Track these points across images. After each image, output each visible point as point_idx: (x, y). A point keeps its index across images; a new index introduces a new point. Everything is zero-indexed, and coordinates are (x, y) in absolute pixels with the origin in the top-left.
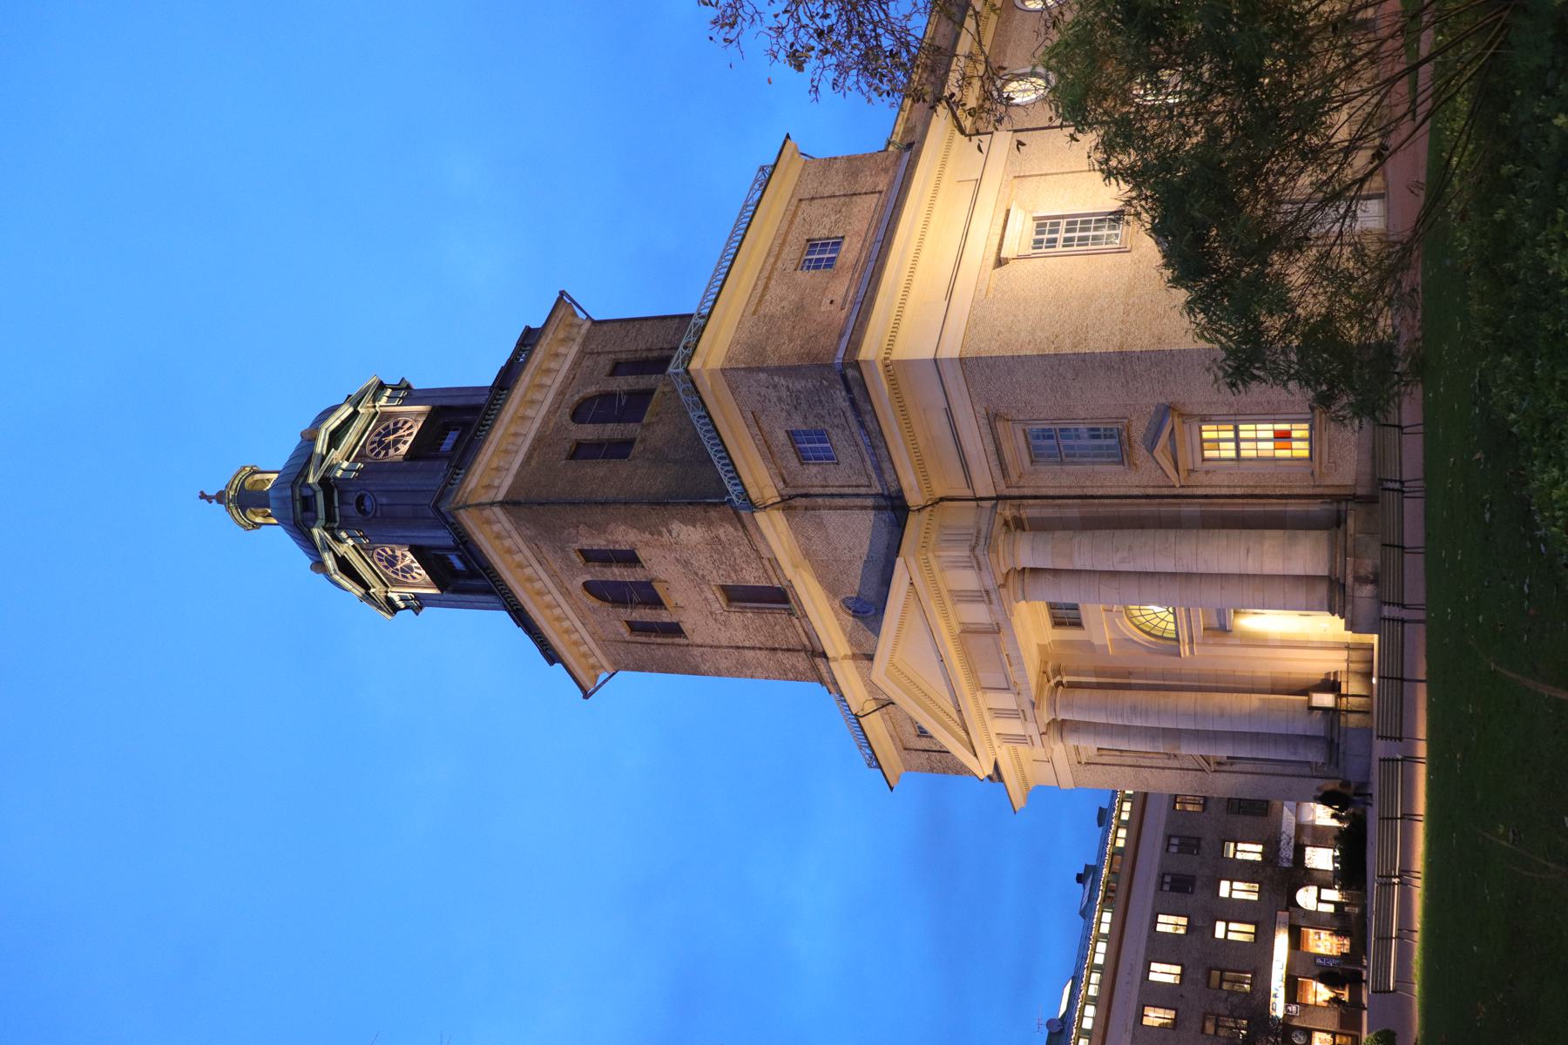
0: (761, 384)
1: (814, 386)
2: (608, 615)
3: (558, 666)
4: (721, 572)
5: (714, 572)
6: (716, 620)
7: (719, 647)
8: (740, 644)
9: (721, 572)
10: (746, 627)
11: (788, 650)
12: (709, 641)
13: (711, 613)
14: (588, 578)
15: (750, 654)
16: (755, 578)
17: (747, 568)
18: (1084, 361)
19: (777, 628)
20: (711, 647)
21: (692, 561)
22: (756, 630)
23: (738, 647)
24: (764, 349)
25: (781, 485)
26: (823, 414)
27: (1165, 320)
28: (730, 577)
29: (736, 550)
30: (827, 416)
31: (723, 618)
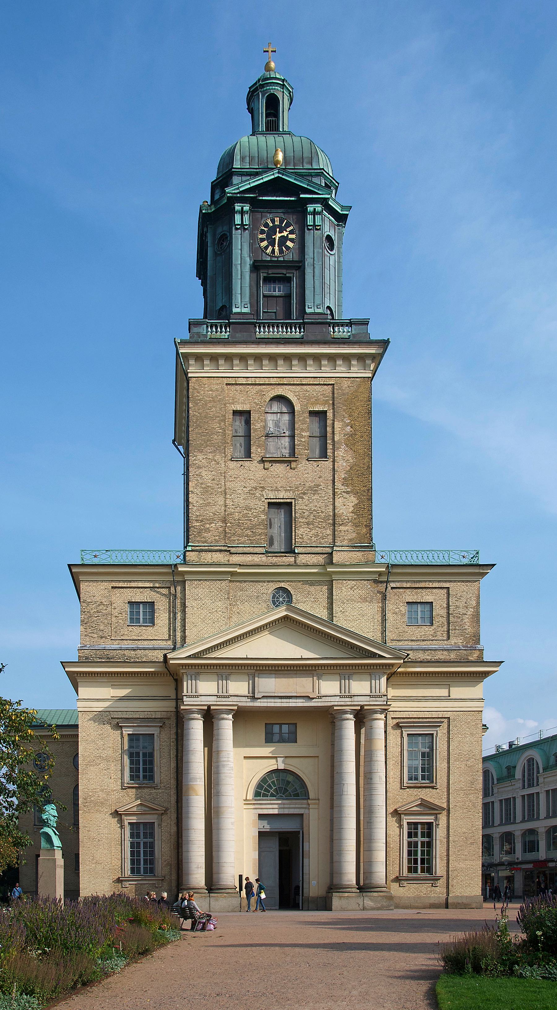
0: (469, 600)
1: (465, 629)
2: (255, 403)
8: (228, 496)
10: (248, 508)
14: (297, 408)
16: (302, 535)
17: (311, 533)
21: (316, 497)
22: (245, 516)
23: (226, 494)
25: (393, 585)
26: (444, 628)
28: (303, 517)
30: (442, 630)
31: (257, 495)
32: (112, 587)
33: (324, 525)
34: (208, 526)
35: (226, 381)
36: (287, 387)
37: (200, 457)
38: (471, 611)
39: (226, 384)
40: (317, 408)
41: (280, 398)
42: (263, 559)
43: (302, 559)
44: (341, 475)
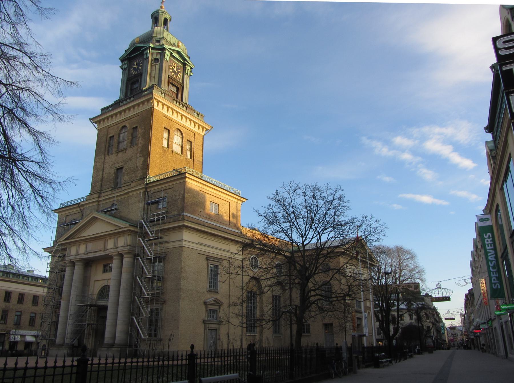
3: (100, 112)
4: (127, 169)
5: (127, 167)
6: (113, 165)
7: (104, 164)
8: (104, 170)
9: (127, 169)
10: (110, 173)
11: (101, 185)
12: (106, 161)
13: (115, 164)
15: (101, 173)
18: (179, 279)
19: (109, 183)
20: (104, 162)
23: (103, 170)
24: (190, 193)
25: (152, 192)
27: (188, 301)
29: (134, 175)
31: (113, 167)
32: (67, 216)
33: (132, 172)
34: (96, 184)
35: (108, 127)
36: (126, 122)
37: (97, 158)
38: (181, 197)
39: (108, 128)
40: (134, 126)
41: (125, 127)
42: (110, 192)
43: (123, 189)
44: (139, 150)
